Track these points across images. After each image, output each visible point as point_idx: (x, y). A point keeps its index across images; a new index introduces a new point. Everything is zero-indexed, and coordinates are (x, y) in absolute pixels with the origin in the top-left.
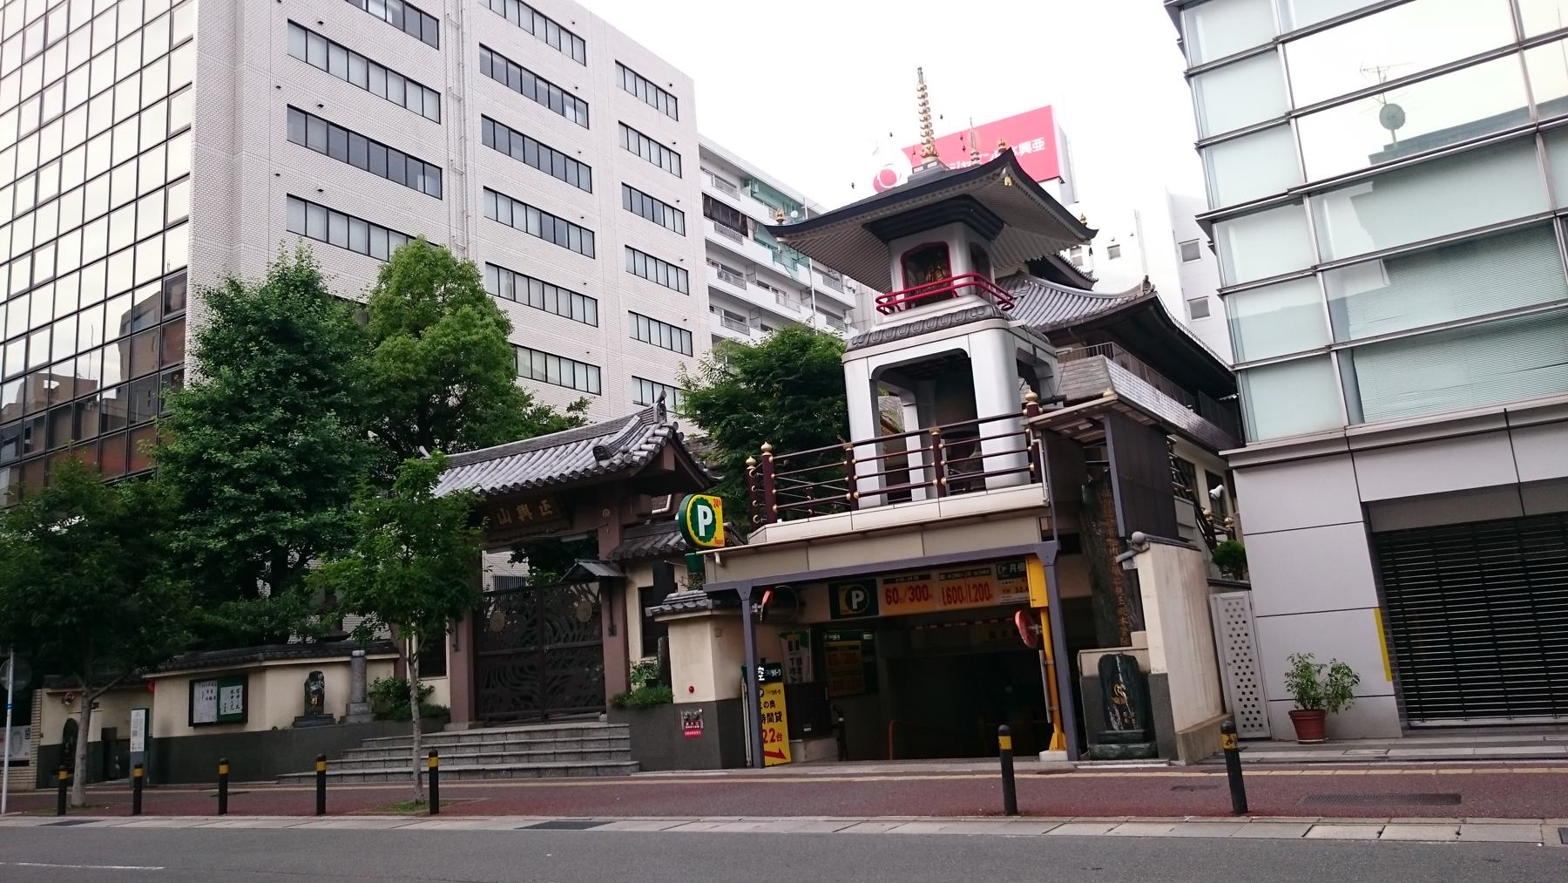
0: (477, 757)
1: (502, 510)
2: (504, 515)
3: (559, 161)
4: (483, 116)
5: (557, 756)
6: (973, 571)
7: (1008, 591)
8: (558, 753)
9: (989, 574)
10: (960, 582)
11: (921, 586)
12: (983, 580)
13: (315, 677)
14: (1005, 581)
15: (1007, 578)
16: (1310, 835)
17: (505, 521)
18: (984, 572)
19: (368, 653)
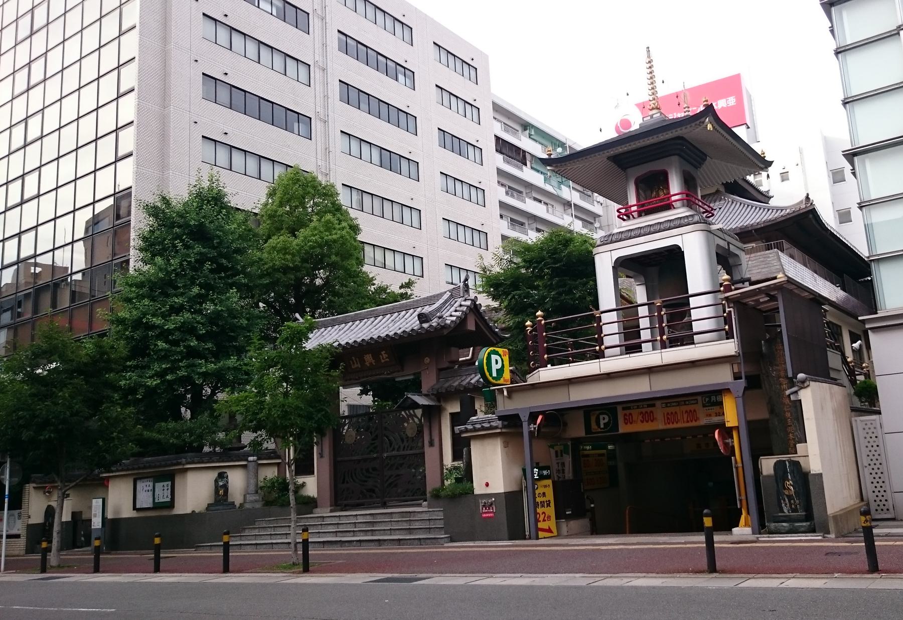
0: (336, 532)
1: (353, 358)
3: (393, 112)
4: (340, 81)
6: (685, 401)
7: (710, 415)
8: (393, 529)
9: (697, 403)
10: (677, 409)
11: (649, 412)
12: (692, 407)
13: (222, 476)
14: (707, 408)
17: (356, 366)
18: (693, 402)
19: (259, 459)
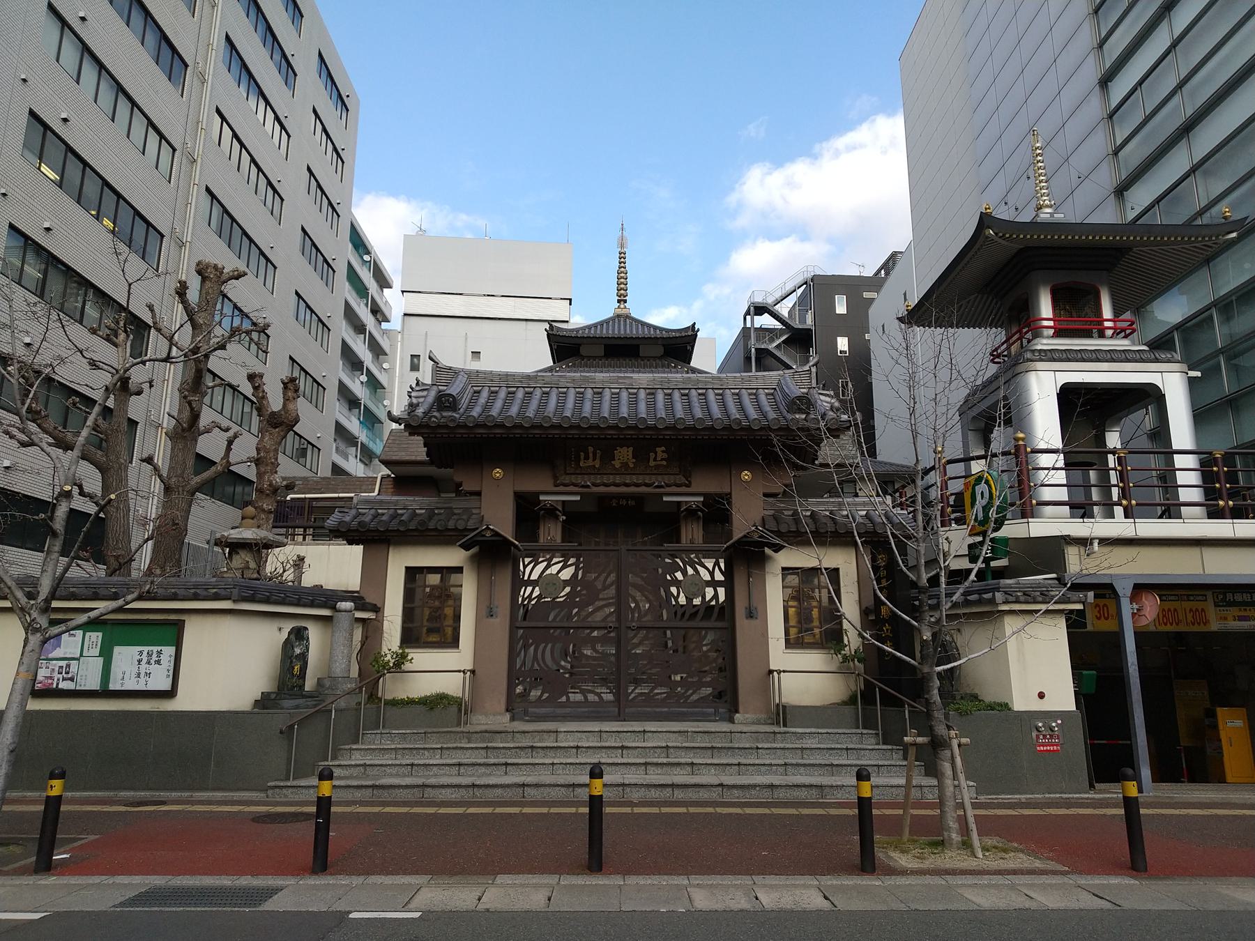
0: (646, 764)
1: (591, 449)
2: (591, 455)
3: (92, 188)
4: (32, 113)
5: (789, 769)
6: (1188, 596)
7: (1226, 619)
8: (792, 765)
9: (1206, 600)
10: (1176, 605)
11: (1101, 605)
12: (1200, 605)
13: (299, 635)
14: (1222, 608)
15: (1223, 606)
16: (467, 812)
17: (590, 462)
18: (1200, 598)
19: (357, 609)
